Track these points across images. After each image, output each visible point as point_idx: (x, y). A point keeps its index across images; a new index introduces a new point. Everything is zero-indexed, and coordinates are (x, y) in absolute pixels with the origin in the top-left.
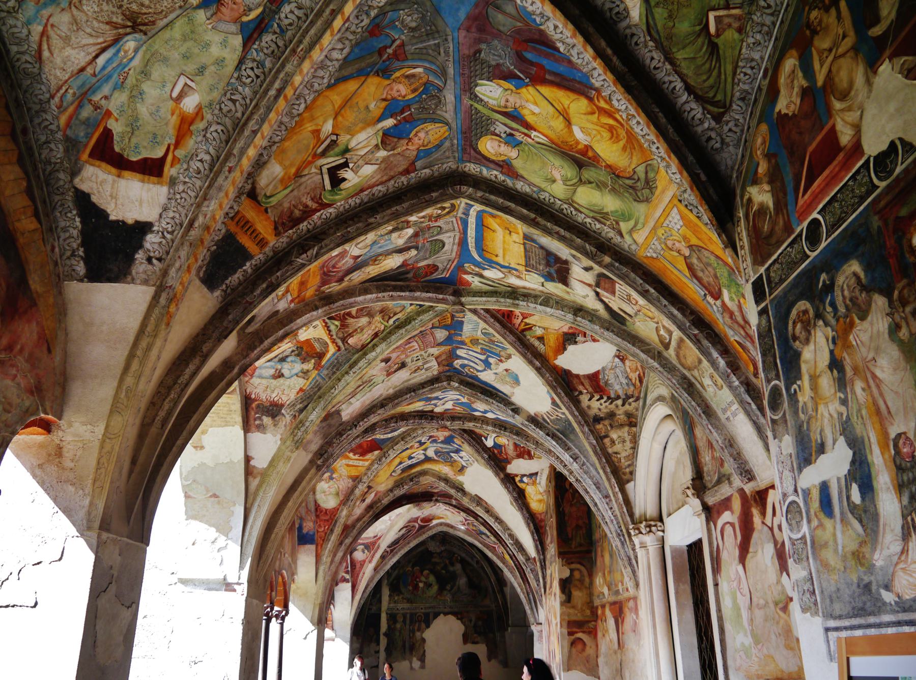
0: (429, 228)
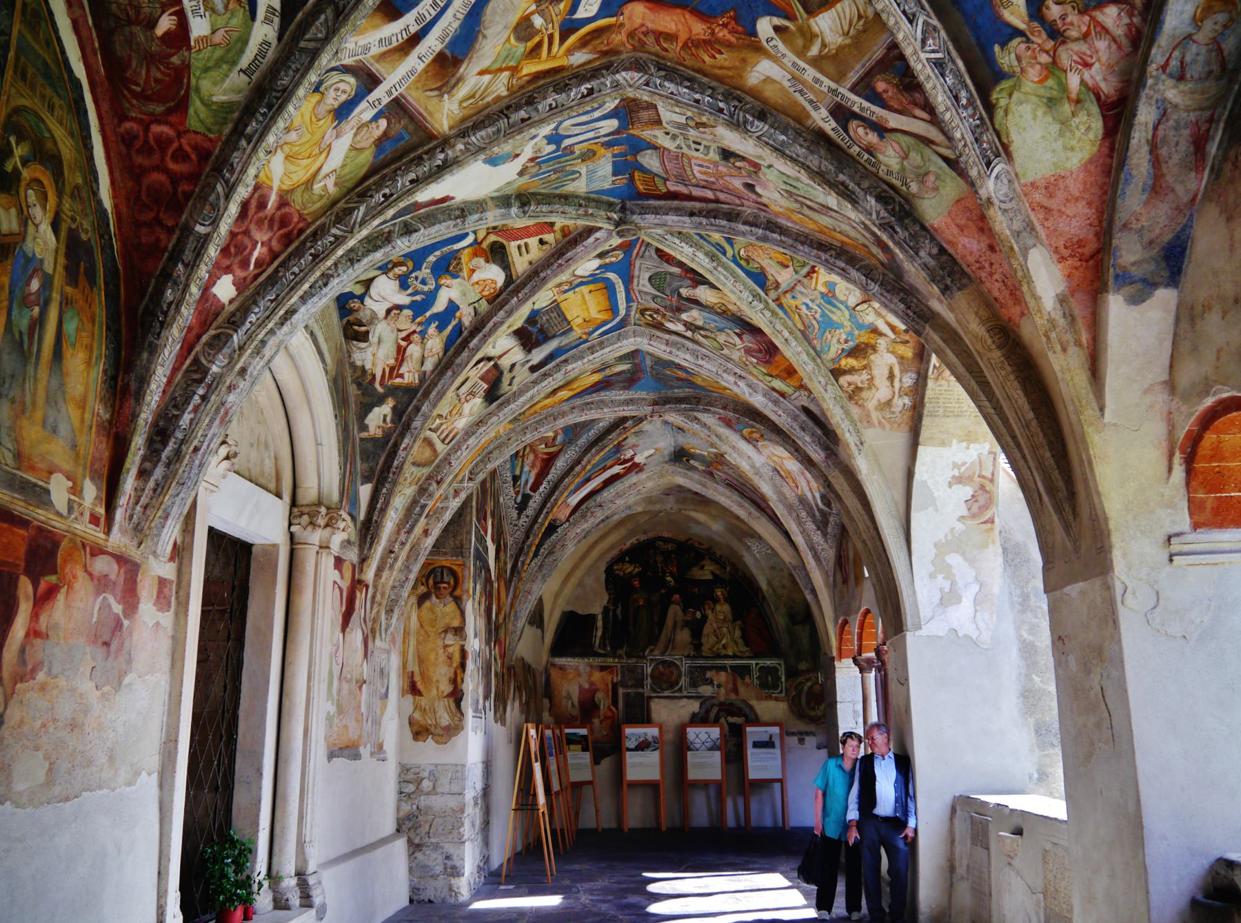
0: (665, 307)
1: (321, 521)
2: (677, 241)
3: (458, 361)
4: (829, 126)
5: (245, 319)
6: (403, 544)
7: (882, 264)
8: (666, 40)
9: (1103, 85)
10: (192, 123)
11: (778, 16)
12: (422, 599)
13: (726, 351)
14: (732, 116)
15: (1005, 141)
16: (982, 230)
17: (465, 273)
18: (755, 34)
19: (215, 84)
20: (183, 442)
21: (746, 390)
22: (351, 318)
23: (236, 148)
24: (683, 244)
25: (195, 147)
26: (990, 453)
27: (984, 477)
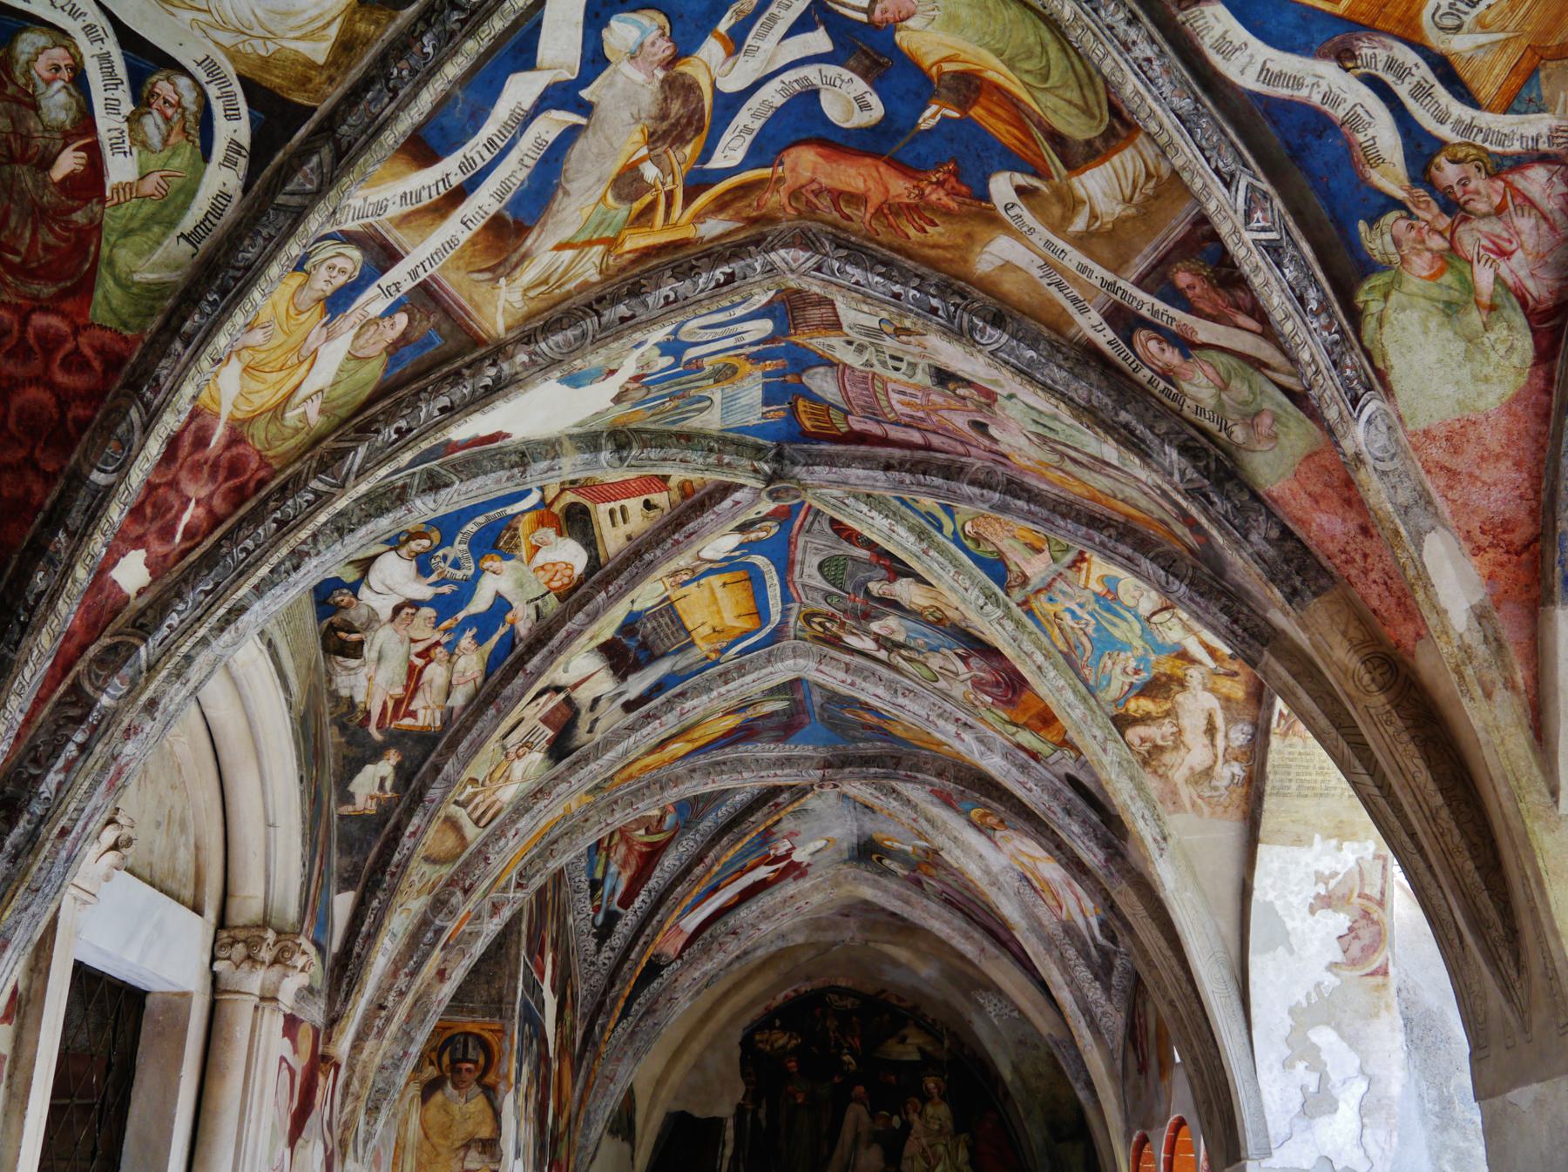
0: (845, 612)
1: (266, 954)
2: (865, 509)
3: (507, 692)
4: (1104, 338)
5: (162, 620)
6: (402, 994)
7: (1191, 551)
8: (848, 203)
9: (1530, 284)
10: (99, 312)
11: (1021, 172)
12: (429, 1090)
13: (942, 684)
14: (950, 318)
15: (1380, 365)
16: (1348, 502)
17: (524, 552)
18: (986, 197)
19: (139, 255)
20: (42, 820)
21: (975, 746)
22: (335, 619)
23: (165, 354)
24: (874, 514)
25: (101, 351)
26: (1377, 857)
27: (1369, 898)
